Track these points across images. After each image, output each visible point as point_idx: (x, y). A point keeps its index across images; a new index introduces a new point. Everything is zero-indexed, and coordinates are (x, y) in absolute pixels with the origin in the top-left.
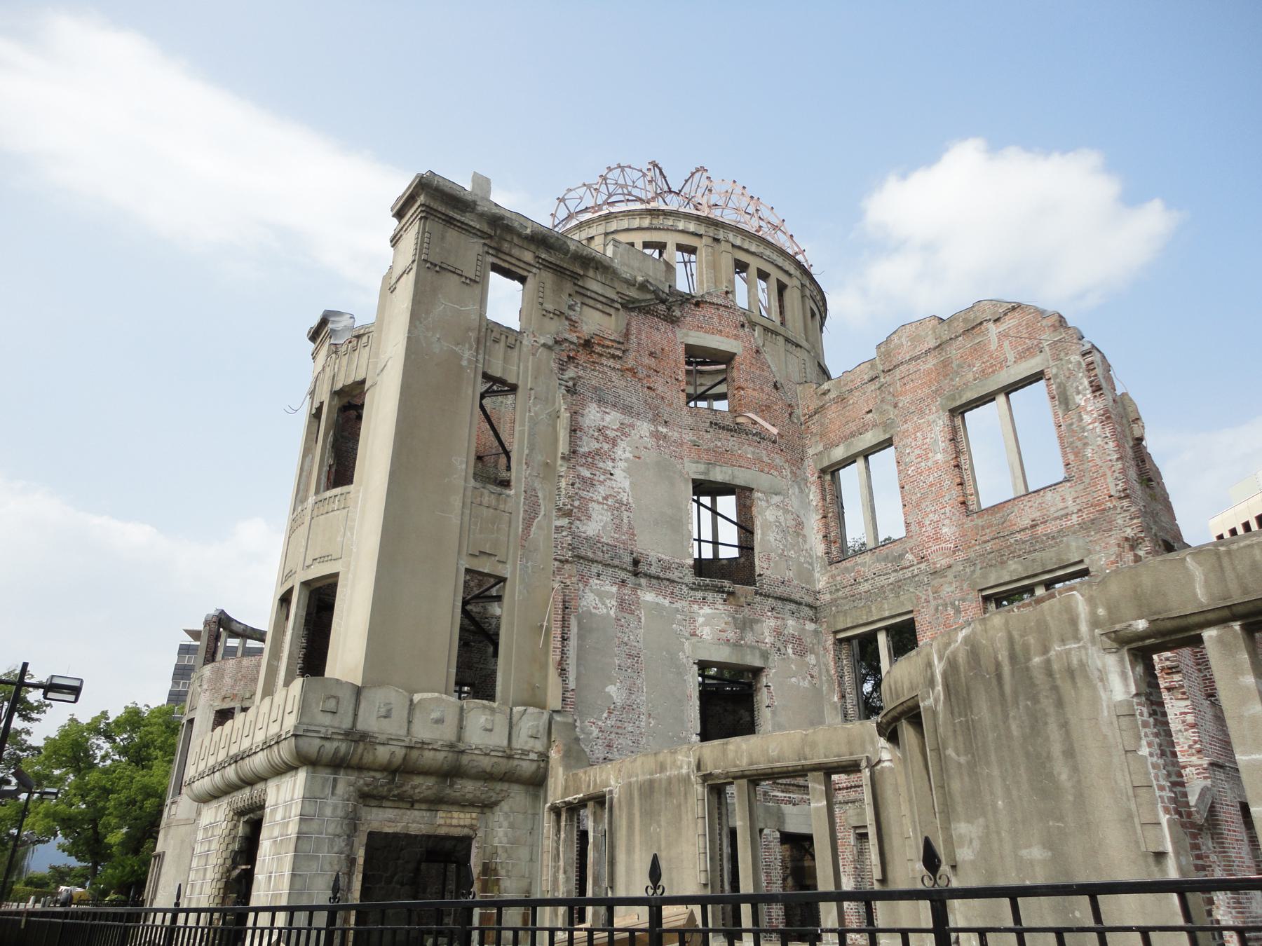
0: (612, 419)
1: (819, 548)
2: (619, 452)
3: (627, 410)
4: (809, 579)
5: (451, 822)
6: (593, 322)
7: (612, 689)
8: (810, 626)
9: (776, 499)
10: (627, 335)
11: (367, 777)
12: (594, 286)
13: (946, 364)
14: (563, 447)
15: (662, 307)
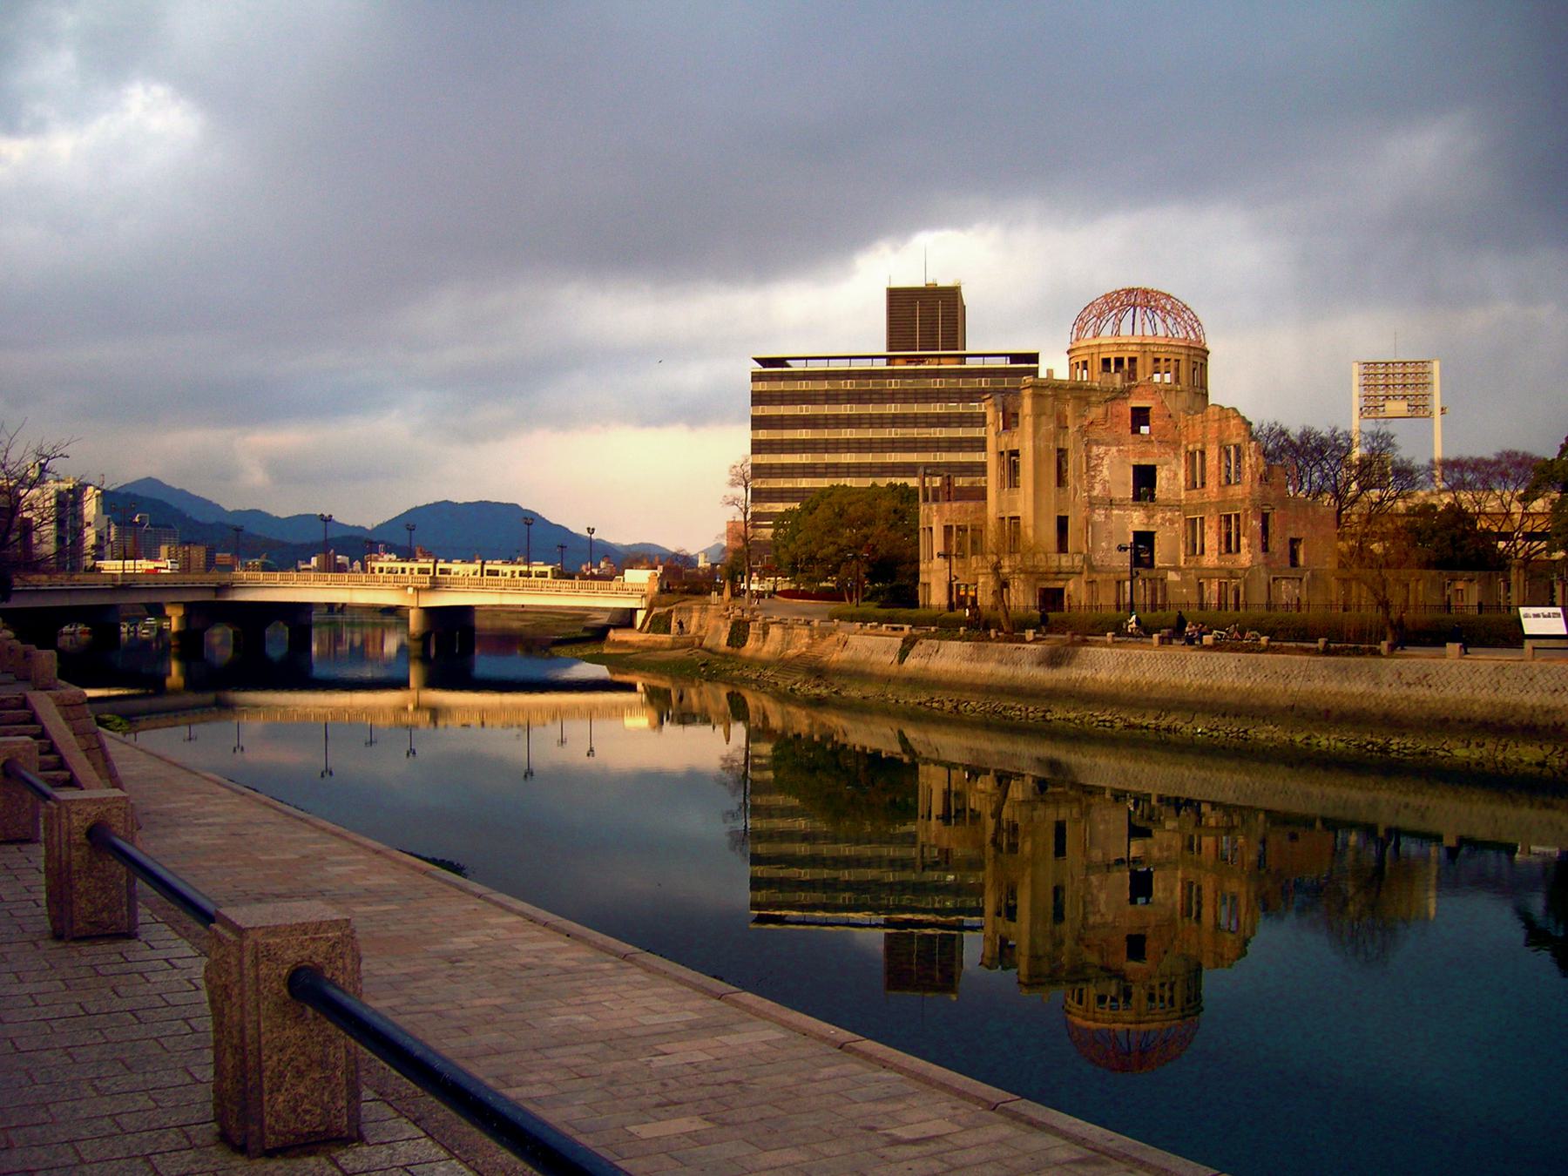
0: (1102, 449)
1: (1183, 483)
2: (1105, 462)
3: (1107, 444)
4: (1179, 495)
5: (1060, 584)
6: (1096, 413)
7: (1103, 544)
8: (1177, 513)
9: (1166, 467)
10: (1107, 414)
11: (1037, 576)
12: (1093, 399)
13: (1220, 426)
14: (1085, 470)
15: (1121, 395)
